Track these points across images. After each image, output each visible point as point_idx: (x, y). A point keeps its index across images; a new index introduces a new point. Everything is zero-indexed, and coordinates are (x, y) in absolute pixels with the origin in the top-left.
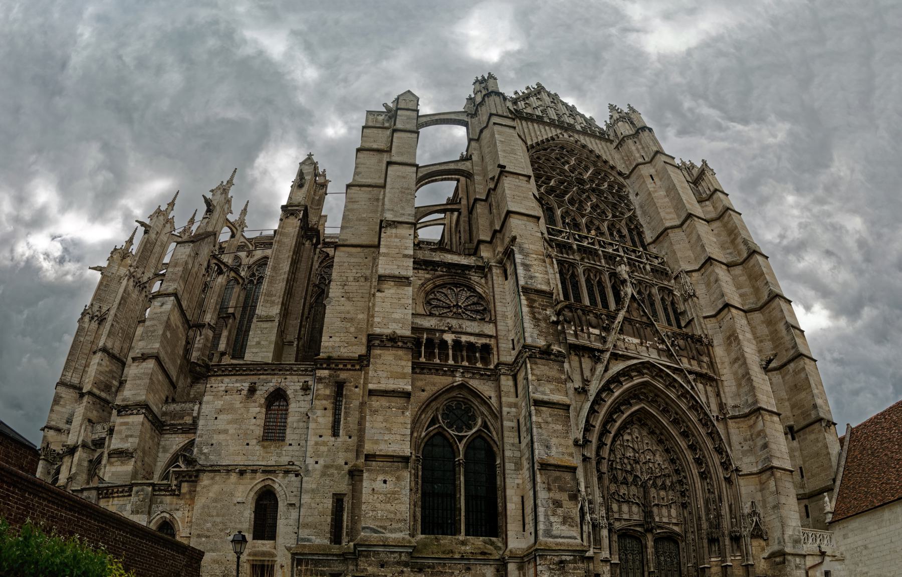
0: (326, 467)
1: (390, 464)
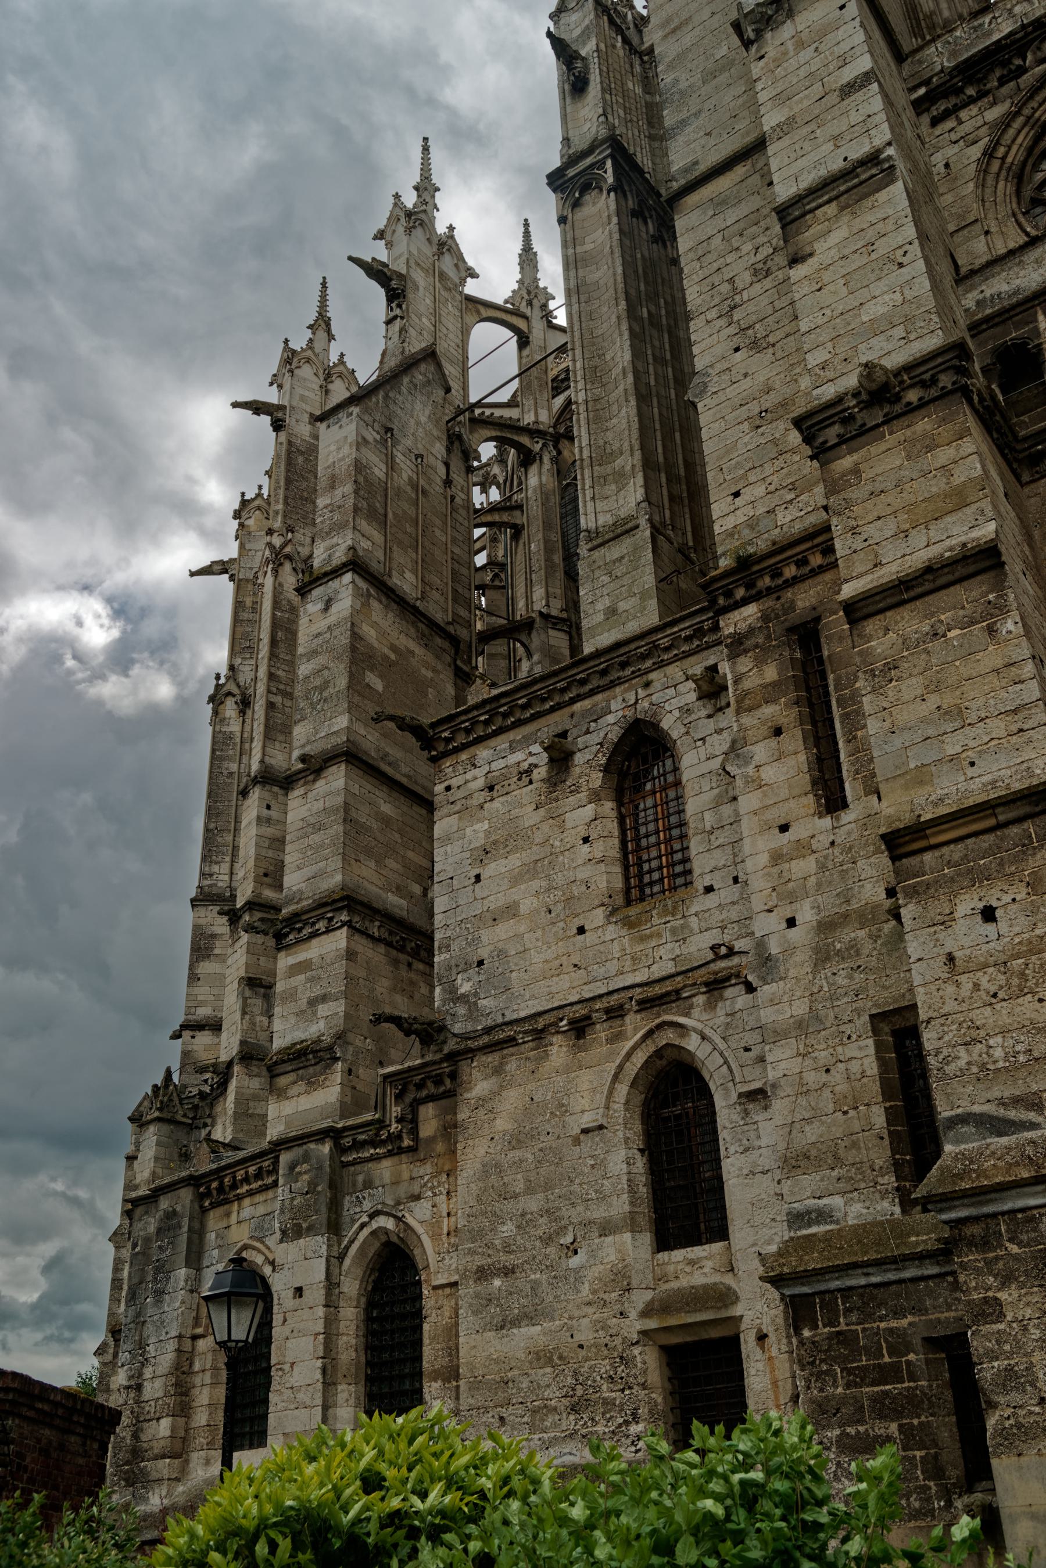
0: (826, 926)
1: (990, 839)
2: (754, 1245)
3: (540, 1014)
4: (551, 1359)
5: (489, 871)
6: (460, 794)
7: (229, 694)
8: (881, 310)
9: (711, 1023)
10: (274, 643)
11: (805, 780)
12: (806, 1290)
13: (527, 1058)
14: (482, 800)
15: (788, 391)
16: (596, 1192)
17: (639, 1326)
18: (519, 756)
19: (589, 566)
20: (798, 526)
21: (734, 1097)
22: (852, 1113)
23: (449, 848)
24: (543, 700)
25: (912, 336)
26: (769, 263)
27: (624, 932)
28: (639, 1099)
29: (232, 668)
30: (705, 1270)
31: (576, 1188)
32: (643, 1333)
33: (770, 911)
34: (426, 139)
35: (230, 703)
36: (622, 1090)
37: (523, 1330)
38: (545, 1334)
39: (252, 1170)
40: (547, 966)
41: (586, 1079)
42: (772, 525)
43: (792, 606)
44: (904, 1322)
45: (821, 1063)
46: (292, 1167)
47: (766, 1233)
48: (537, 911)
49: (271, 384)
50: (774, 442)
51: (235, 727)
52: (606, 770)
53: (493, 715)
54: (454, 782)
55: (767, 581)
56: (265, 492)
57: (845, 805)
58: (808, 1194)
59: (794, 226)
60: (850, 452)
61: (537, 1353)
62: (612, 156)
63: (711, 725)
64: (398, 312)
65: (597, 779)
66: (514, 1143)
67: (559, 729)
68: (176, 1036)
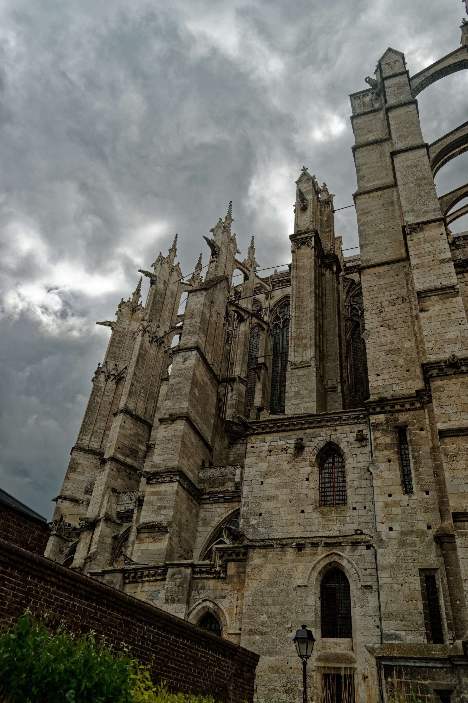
0: (404, 534)
2: (364, 642)
3: (284, 539)
4: (278, 671)
5: (266, 481)
6: (257, 450)
7: (103, 372)
8: (453, 337)
9: (352, 557)
10: (138, 361)
11: (399, 480)
12: (390, 663)
13: (277, 554)
14: (266, 455)
15: (400, 346)
16: (302, 610)
17: (316, 664)
18: (282, 442)
19: (291, 374)
20: (400, 393)
21: (359, 586)
22: (410, 602)
23: (251, 469)
24: (295, 425)
25: (464, 348)
26: (395, 301)
27: (320, 516)
28: (320, 579)
29: (106, 362)
30: (341, 648)
31: (293, 607)
32: (318, 668)
33: (383, 523)
34: (231, 202)
35: (103, 375)
36: (315, 574)
37: (267, 657)
38: (276, 660)
39: (152, 572)
40: (288, 522)
41: (300, 567)
42: (391, 389)
43: (397, 419)
44: (427, 682)
45: (400, 582)
46: (173, 575)
47: (369, 639)
48: (286, 501)
49: (152, 266)
50: (394, 362)
51: (102, 385)
52: (317, 456)
53: (275, 425)
54: (255, 445)
55: (389, 408)
56: (131, 300)
57: (412, 492)
58: (392, 628)
59: (422, 299)
60: (441, 380)
61: (272, 667)
62: (314, 236)
63: (359, 451)
64: (216, 259)
65: (313, 459)
66: (269, 585)
67: (300, 437)
68: (56, 500)
